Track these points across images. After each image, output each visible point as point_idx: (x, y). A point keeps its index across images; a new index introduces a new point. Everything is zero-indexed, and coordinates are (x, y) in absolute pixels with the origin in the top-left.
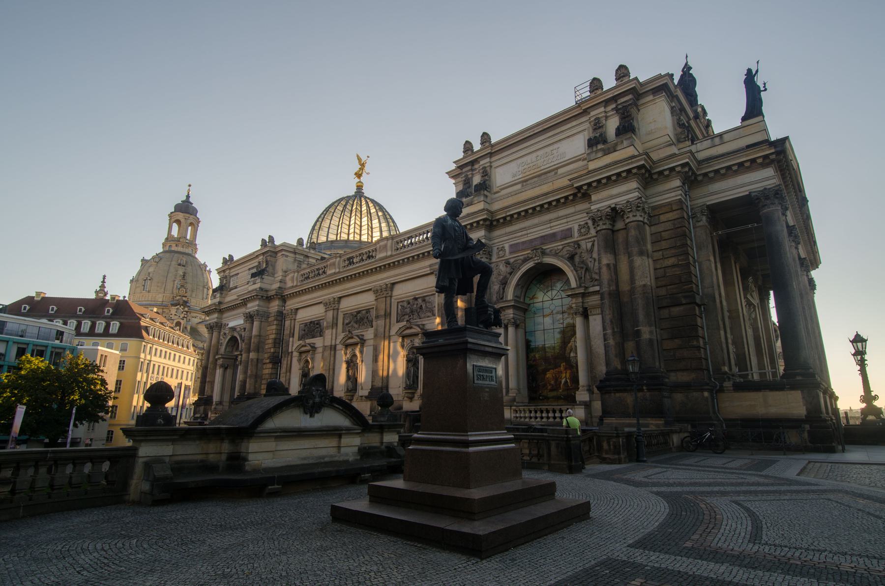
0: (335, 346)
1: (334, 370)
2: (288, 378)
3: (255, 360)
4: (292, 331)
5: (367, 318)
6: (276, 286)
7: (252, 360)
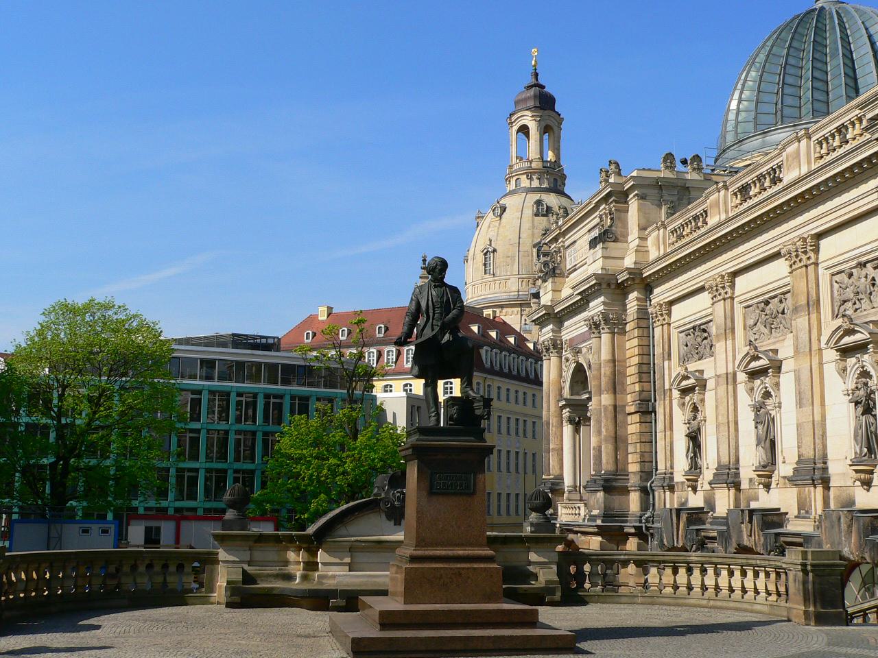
0: (735, 374)
1: (736, 423)
2: (668, 440)
3: (611, 408)
4: (667, 347)
5: (783, 313)
6: (629, 262)
7: (606, 407)
